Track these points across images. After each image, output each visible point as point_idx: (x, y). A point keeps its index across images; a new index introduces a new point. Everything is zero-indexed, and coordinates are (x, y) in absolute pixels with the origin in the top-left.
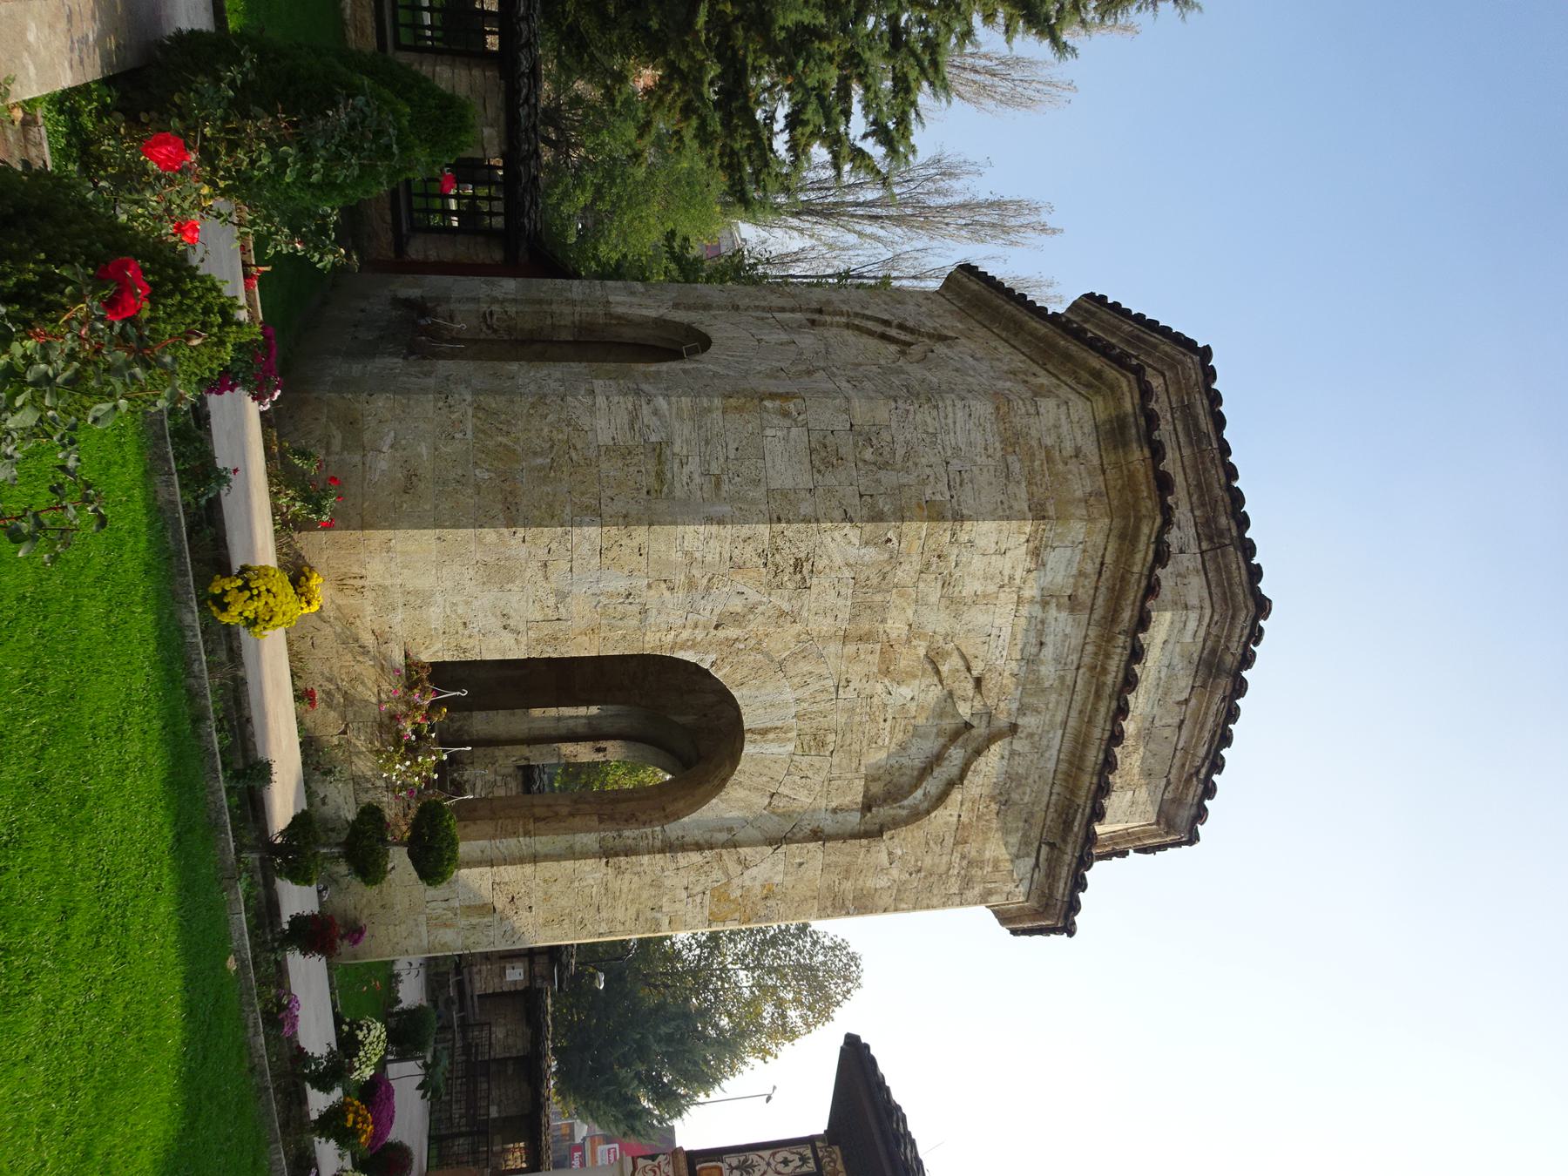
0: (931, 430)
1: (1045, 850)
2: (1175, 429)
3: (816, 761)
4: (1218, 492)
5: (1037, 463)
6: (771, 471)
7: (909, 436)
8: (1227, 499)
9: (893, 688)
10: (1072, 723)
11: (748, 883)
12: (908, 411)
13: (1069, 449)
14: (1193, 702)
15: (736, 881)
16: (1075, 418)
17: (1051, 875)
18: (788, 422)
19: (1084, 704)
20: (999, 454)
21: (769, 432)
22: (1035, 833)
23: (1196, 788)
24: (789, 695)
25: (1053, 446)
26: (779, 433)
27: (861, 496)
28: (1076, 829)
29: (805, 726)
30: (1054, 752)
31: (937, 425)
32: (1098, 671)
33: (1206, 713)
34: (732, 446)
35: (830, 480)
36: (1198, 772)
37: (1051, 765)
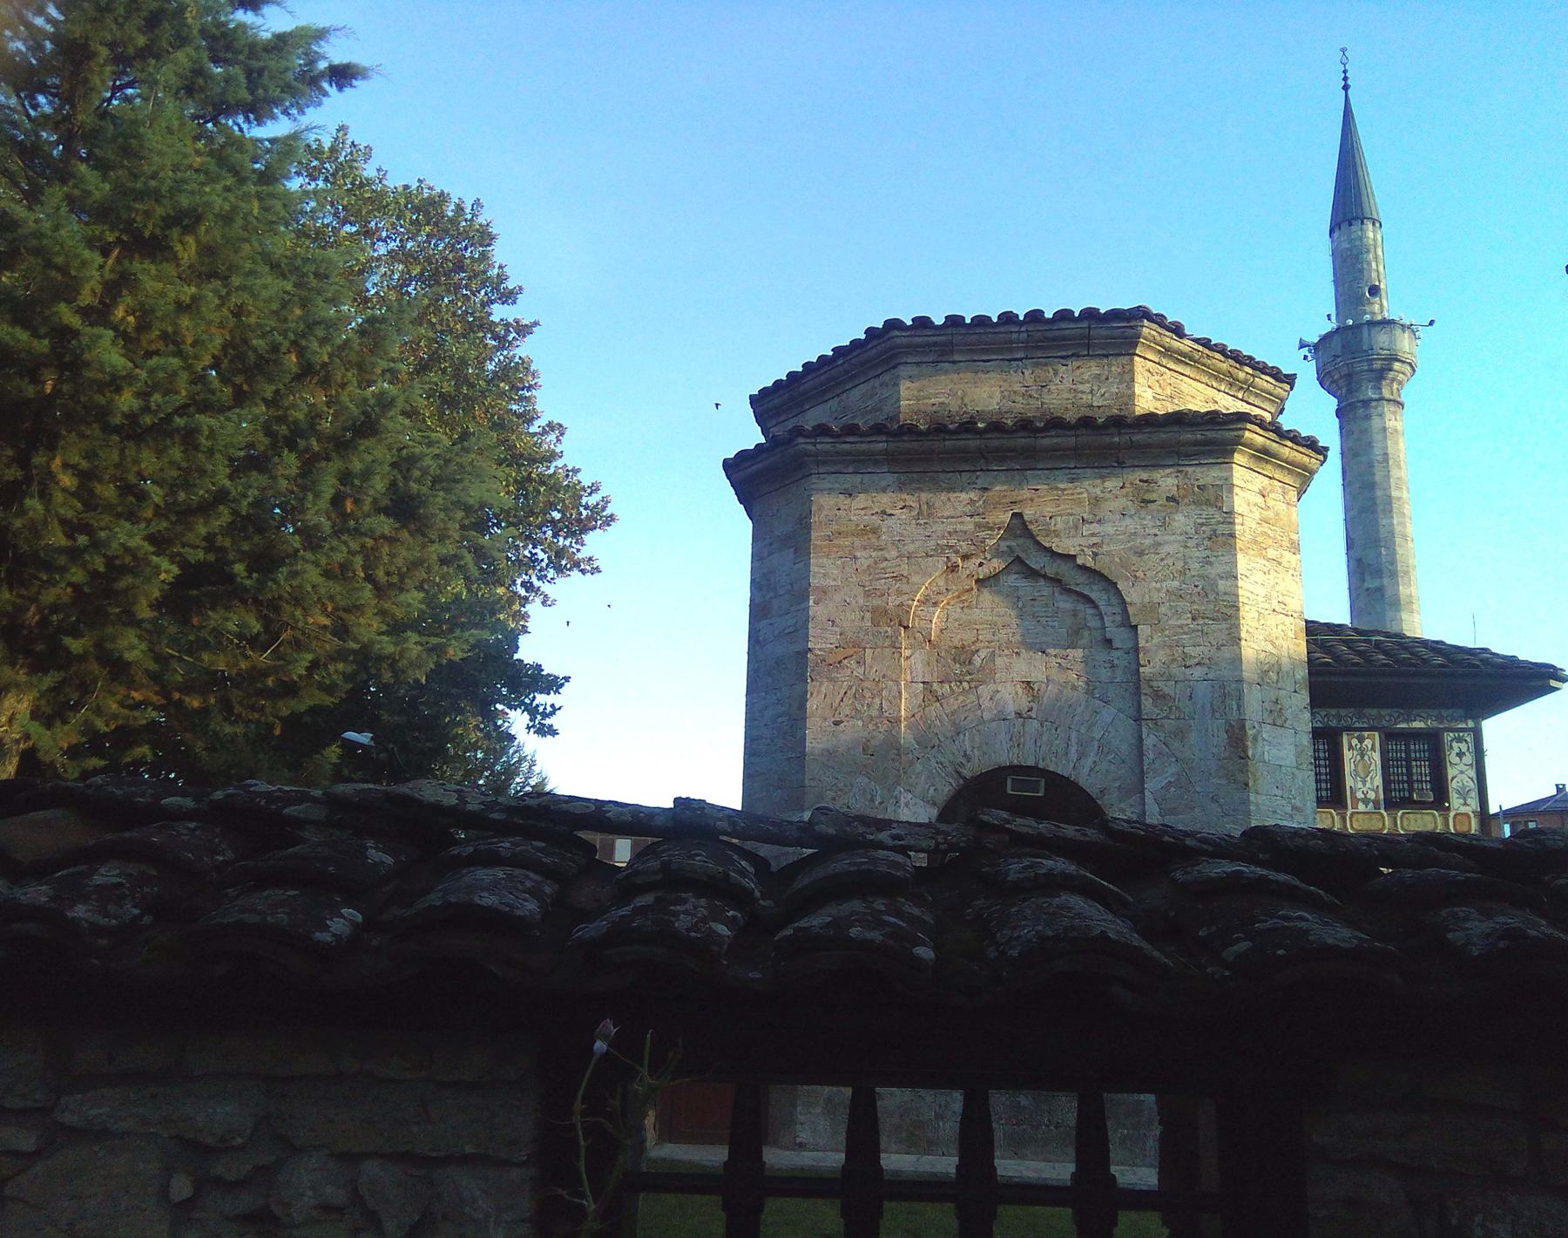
0: (1256, 615)
2: (1170, 370)
4: (1224, 366)
5: (1269, 532)
6: (1288, 762)
7: (1261, 637)
8: (1232, 362)
12: (1247, 631)
13: (1259, 500)
16: (1243, 485)
18: (1260, 738)
20: (1267, 563)
21: (1266, 758)
25: (1261, 513)
26: (1267, 748)
27: (1295, 692)
31: (1254, 609)
34: (1276, 792)
35: (1288, 713)
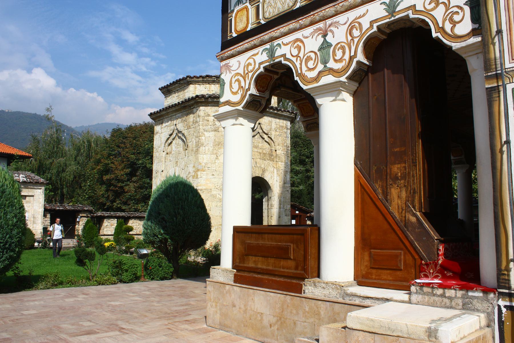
1: (192, 108)
3: (179, 162)
9: (173, 150)
10: (174, 114)
11: (192, 171)
14: (174, 91)
15: (192, 174)
17: (193, 105)
19: (171, 114)
22: (190, 111)
23: (182, 82)
24: (171, 170)
28: (183, 105)
29: (174, 166)
30: (178, 115)
32: (167, 114)
33: (173, 88)
36: (179, 83)
37: (180, 114)
